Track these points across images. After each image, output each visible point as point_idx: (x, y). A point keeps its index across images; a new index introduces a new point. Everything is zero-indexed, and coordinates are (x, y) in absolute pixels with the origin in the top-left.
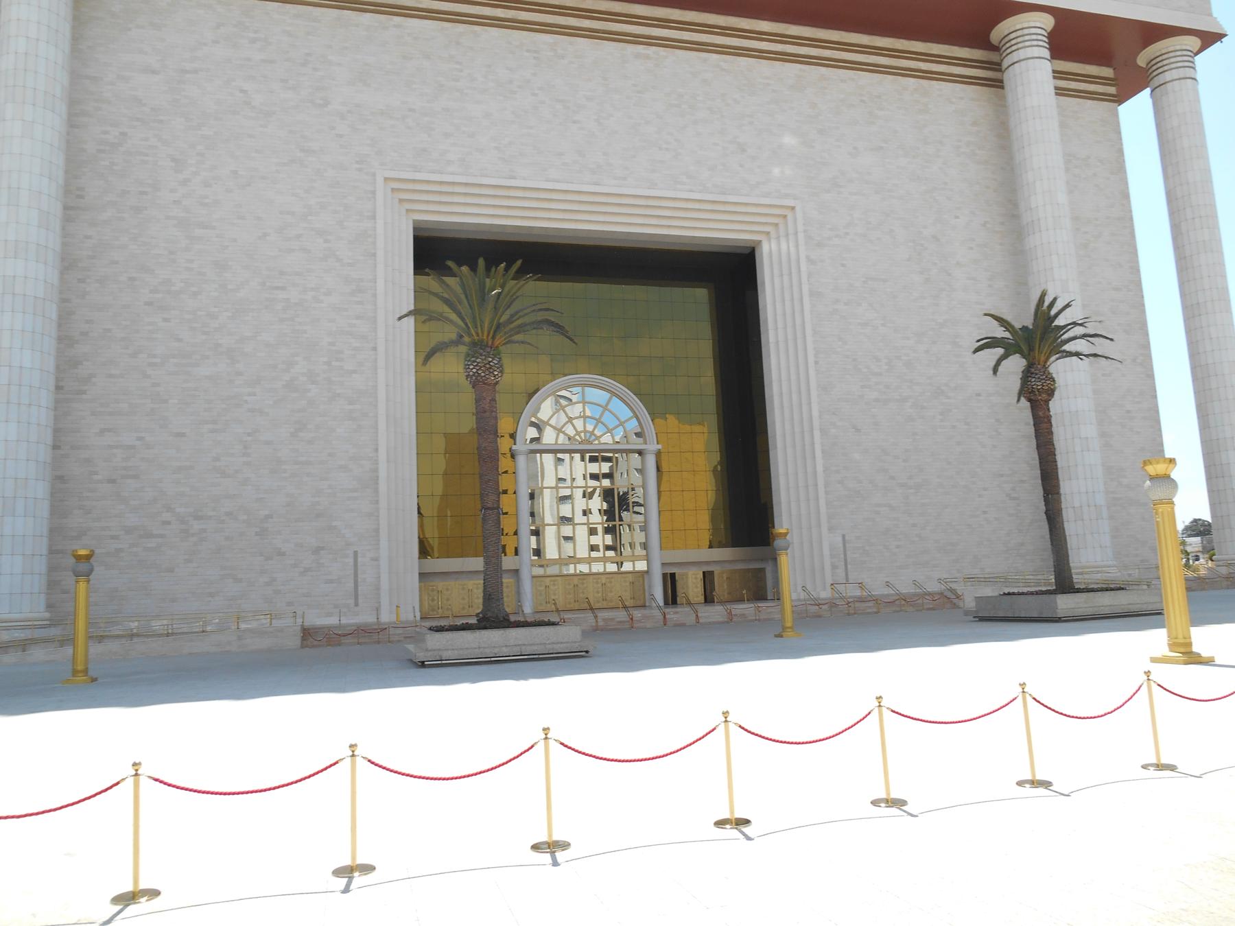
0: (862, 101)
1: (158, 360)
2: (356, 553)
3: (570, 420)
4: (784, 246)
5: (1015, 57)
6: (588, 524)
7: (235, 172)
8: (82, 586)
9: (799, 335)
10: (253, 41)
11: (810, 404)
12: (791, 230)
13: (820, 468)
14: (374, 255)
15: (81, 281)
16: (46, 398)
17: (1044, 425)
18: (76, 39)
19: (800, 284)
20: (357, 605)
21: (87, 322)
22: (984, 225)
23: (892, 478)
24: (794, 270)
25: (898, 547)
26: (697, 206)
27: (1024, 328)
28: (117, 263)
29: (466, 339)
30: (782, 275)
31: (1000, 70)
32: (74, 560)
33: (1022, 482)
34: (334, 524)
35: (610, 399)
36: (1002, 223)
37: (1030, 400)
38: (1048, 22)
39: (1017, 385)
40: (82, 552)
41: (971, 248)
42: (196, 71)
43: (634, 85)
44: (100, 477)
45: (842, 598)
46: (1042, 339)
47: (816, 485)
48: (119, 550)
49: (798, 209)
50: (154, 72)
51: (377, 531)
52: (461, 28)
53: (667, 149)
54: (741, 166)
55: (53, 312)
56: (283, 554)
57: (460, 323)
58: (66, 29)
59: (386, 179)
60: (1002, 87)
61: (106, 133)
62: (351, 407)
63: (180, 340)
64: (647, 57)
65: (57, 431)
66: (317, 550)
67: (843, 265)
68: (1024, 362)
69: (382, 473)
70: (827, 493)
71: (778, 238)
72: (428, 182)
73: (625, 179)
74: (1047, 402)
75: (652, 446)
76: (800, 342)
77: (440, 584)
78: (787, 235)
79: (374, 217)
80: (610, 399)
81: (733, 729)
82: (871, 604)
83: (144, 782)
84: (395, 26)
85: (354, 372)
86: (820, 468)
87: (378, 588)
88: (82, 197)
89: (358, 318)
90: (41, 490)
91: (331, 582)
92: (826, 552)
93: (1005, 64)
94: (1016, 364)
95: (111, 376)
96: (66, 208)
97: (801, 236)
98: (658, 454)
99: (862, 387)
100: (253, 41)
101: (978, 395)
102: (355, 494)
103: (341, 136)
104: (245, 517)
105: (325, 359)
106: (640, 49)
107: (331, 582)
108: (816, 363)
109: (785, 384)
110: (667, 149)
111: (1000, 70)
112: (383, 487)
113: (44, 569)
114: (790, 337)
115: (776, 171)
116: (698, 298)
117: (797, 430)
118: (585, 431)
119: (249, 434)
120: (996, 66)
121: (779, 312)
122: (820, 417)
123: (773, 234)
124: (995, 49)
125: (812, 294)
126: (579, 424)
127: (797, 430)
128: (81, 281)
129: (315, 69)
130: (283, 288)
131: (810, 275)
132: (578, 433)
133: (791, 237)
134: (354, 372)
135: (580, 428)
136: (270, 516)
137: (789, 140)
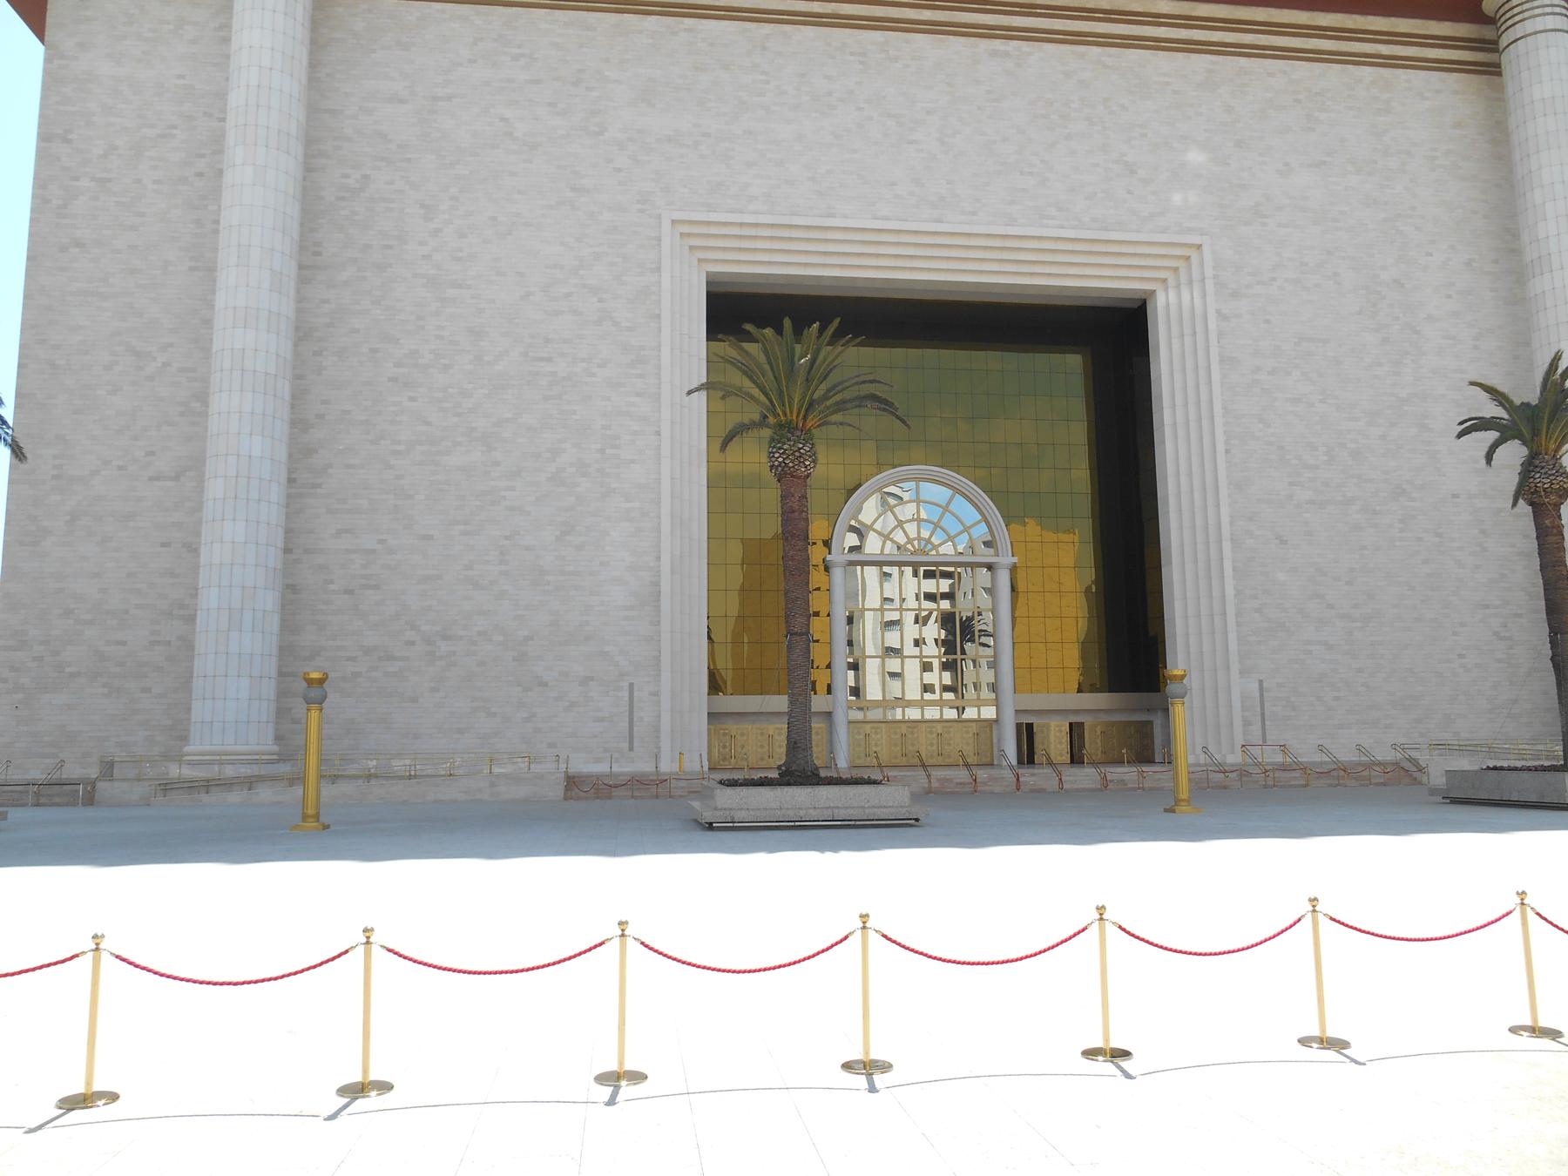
0: (1299, 101)
1: (402, 448)
2: (631, 685)
3: (900, 524)
4: (1186, 297)
5: (1518, 31)
6: (921, 657)
7: (495, 219)
8: (314, 714)
9: (1205, 414)
10: (516, 58)
11: (1218, 506)
13: (1230, 592)
14: (659, 316)
15: (316, 353)
16: (276, 493)
17: (1552, 539)
18: (313, 65)
19: (1208, 348)
20: (631, 749)
21: (324, 402)
22: (1469, 264)
23: (1330, 606)
25: (1337, 699)
26: (1070, 247)
27: (1526, 405)
28: (357, 331)
29: (771, 420)
31: (1496, 50)
32: (305, 684)
33: (1520, 616)
35: (952, 498)
36: (1496, 262)
37: (1531, 504)
39: (1512, 481)
40: (315, 675)
41: (1449, 296)
42: (449, 98)
43: (989, 92)
44: (332, 587)
45: (1258, 764)
46: (1550, 421)
47: (1224, 614)
48: (356, 675)
49: (1206, 248)
50: (402, 101)
51: (658, 659)
52: (767, 28)
53: (1031, 173)
54: (1129, 192)
55: (285, 390)
56: (543, 684)
57: (763, 398)
58: (302, 54)
59: (673, 222)
60: (1499, 74)
61: (346, 176)
63: (428, 423)
64: (1006, 55)
65: (288, 532)
66: (586, 681)
67: (1267, 321)
68: (1525, 451)
69: (665, 587)
70: (1238, 624)
71: (1178, 287)
72: (725, 224)
73: (974, 213)
74: (1557, 506)
76: (1205, 423)
77: (733, 727)
78: (1190, 282)
79: (658, 269)
80: (952, 498)
81: (1111, 930)
82: (1294, 774)
83: (378, 954)
84: (689, 30)
85: (633, 461)
86: (1230, 592)
87: (657, 730)
88: (319, 254)
89: (638, 394)
90: (269, 601)
91: (601, 720)
92: (1237, 703)
93: (1504, 41)
94: (1513, 454)
95: (349, 466)
96: (301, 267)
97: (1209, 284)
98: (1013, 570)
99: (1291, 484)
100: (516, 58)
101: (1456, 496)
103: (620, 170)
106: (997, 44)
107: (601, 720)
108: (1227, 451)
109: (1183, 479)
110: (1031, 173)
111: (1496, 50)
112: (665, 603)
113: (272, 695)
114: (1192, 416)
115: (1177, 198)
116: (1073, 363)
117: (1200, 539)
118: (919, 538)
119: (507, 538)
120: (1491, 46)
121: (1178, 385)
122: (1232, 523)
123: (1171, 282)
124: (1490, 21)
125: (1223, 360)
126: (911, 529)
127: (1200, 539)
128: (316, 353)
129: (589, 89)
130: (549, 360)
131: (1220, 335)
132: (910, 541)
133: (1196, 286)
134: (633, 461)
135: (913, 533)
136: (528, 638)
137: (1195, 157)
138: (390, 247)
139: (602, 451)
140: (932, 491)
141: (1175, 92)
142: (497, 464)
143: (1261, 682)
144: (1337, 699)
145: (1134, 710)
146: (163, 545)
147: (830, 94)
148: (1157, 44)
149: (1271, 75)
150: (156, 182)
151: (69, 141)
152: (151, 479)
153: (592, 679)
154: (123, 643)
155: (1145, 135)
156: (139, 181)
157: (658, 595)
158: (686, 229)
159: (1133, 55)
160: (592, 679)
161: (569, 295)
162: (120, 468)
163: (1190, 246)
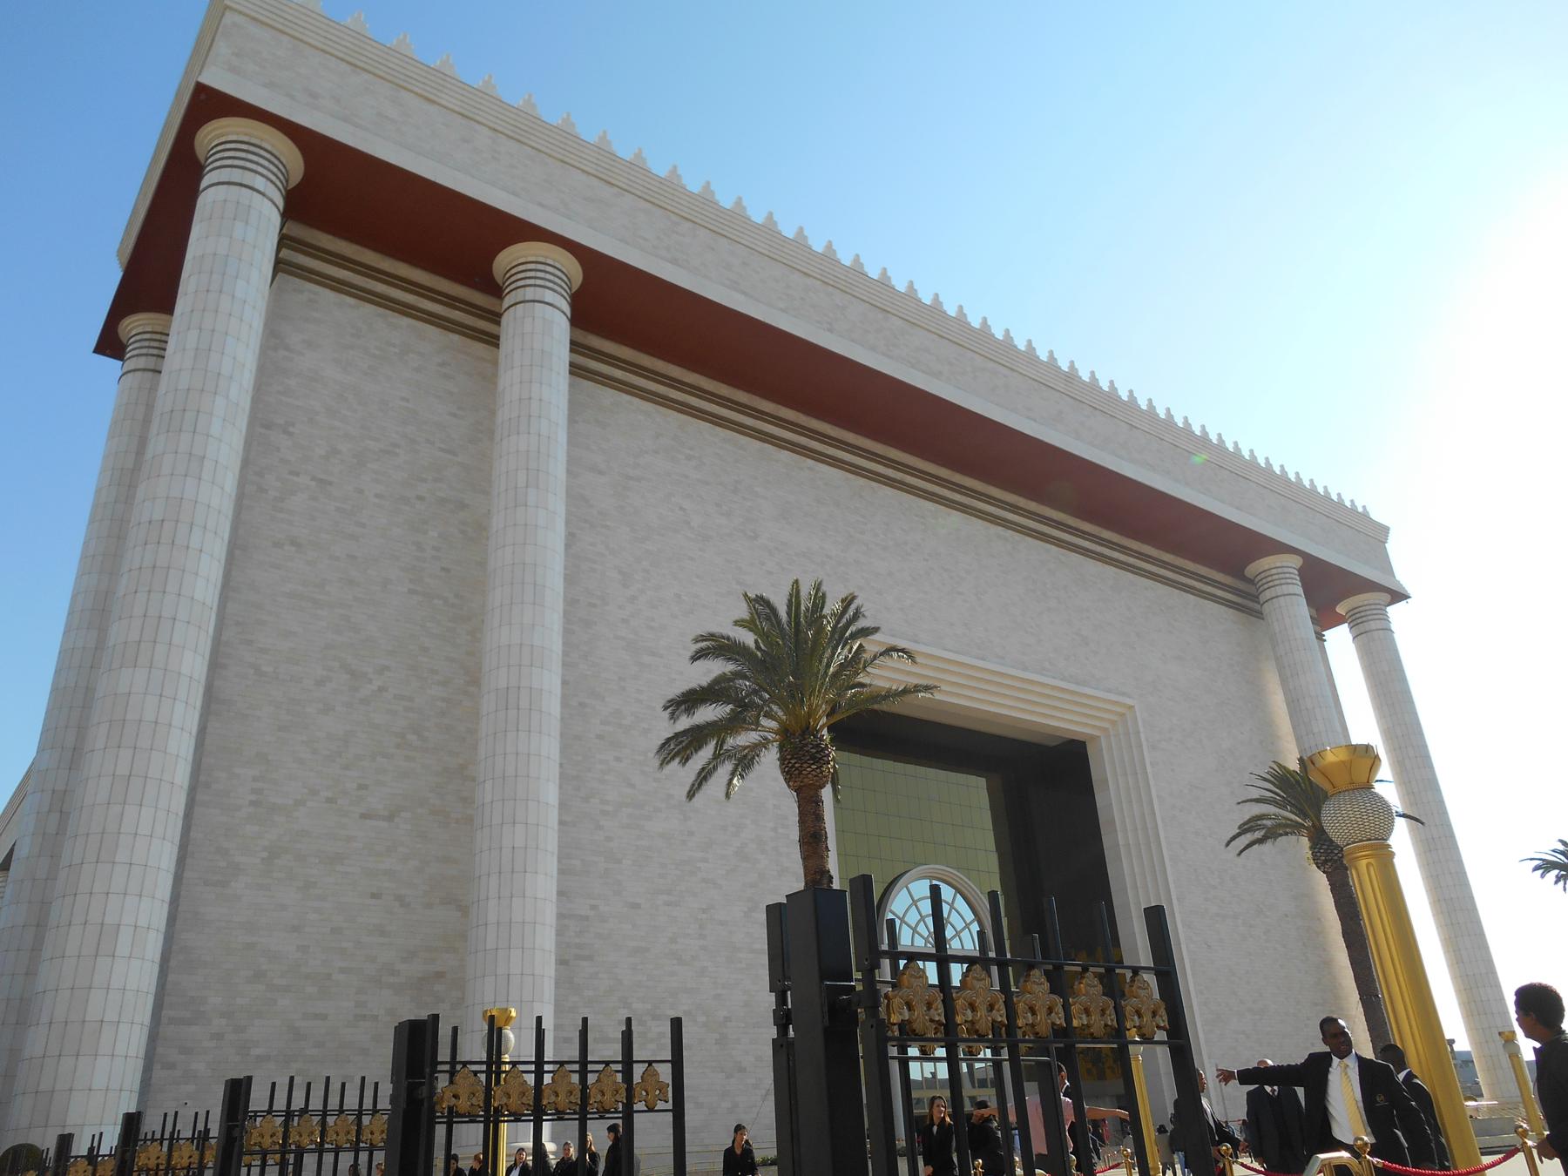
1: (610, 808)
5: (1279, 590)
38: (1296, 561)
50: (601, 473)
52: (862, 481)
56: (742, 1070)
63: (632, 786)
84: (810, 469)
93: (1262, 598)
100: (689, 458)
103: (770, 573)
104: (704, 1019)
119: (704, 911)
120: (1255, 598)
124: (1251, 581)
136: (727, 1019)
138: (594, 606)
139: (775, 829)
142: (691, 833)
146: (374, 896)
148: (1086, 552)
150: (377, 496)
151: (290, 434)
152: (363, 816)
154: (324, 1017)
156: (361, 491)
159: (1076, 558)
162: (329, 800)
163: (1124, 705)
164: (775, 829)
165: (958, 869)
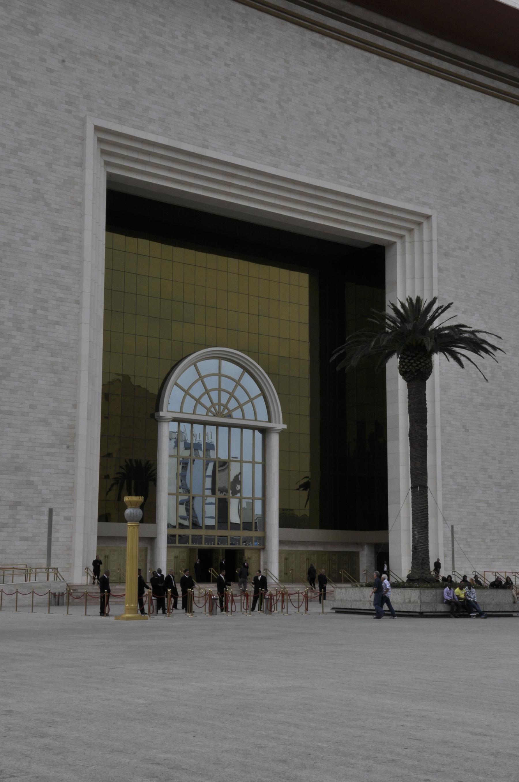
0: (485, 123)
2: (51, 511)
12: (426, 237)
23: (490, 477)
24: (426, 275)
25: (492, 541)
30: (414, 278)
34: (32, 479)
43: (310, 73)
49: (434, 219)
53: (334, 143)
54: (391, 169)
59: (97, 129)
62: (53, 359)
64: (322, 47)
66: (14, 505)
67: (463, 276)
71: (412, 242)
73: (298, 165)
75: (281, 426)
89: (63, 267)
91: (26, 539)
97: (435, 244)
98: (282, 433)
102: (53, 450)
105: (31, 307)
106: (316, 36)
107: (26, 539)
110: (334, 143)
123: (407, 238)
132: (219, 404)
133: (426, 245)
134: (57, 323)
139: (34, 311)
140: (231, 369)
141: (420, 101)
143: (452, 527)
144: (492, 541)
145: (313, 543)
147: (206, 47)
149: (473, 101)
153: (18, 504)
155: (401, 129)
157: (74, 436)
158: (103, 136)
159: (398, 67)
160: (18, 504)
161: (10, 171)
164: (34, 311)
165: (247, 352)
